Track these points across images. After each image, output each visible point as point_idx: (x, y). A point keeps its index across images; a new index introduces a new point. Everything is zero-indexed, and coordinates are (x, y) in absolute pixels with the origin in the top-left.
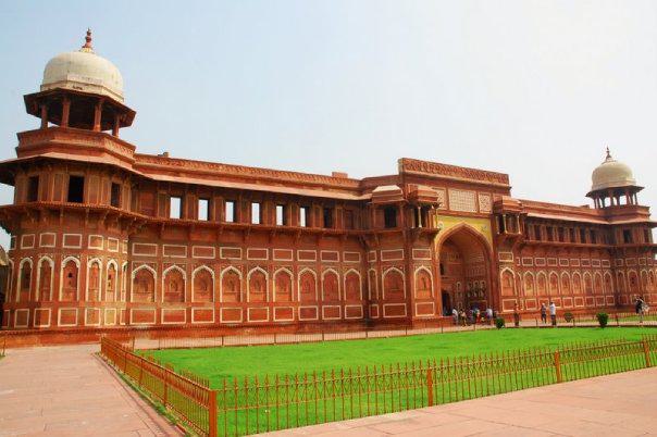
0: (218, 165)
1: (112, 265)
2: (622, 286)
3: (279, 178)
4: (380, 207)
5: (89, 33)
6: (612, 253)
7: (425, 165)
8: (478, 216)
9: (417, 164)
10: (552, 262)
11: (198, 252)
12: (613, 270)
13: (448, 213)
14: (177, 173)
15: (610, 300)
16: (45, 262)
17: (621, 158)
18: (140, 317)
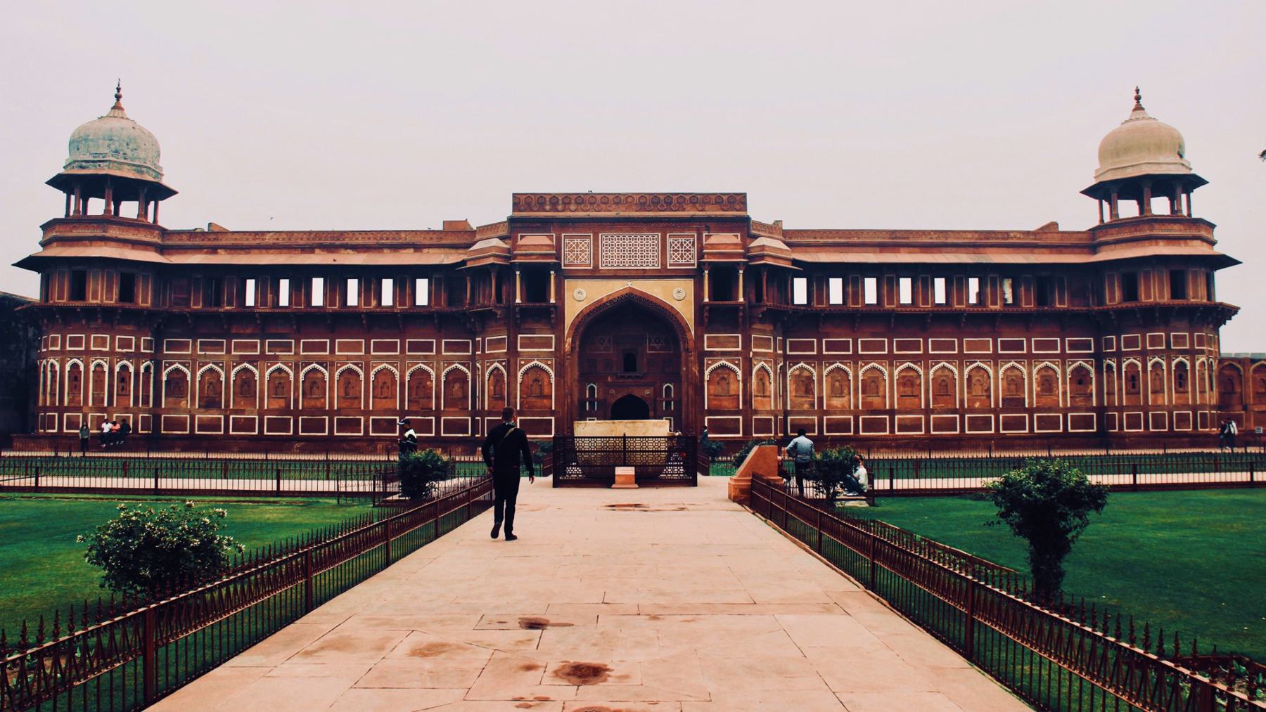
0: (263, 233)
1: (124, 368)
2: (1110, 393)
3: (347, 241)
4: (482, 274)
5: (118, 89)
6: (1097, 325)
7: (554, 200)
8: (663, 274)
9: (540, 200)
10: (901, 346)
11: (239, 347)
12: (1098, 358)
13: (594, 274)
14: (213, 250)
15: (1087, 422)
16: (53, 366)
17: (1159, 111)
18: (171, 424)
